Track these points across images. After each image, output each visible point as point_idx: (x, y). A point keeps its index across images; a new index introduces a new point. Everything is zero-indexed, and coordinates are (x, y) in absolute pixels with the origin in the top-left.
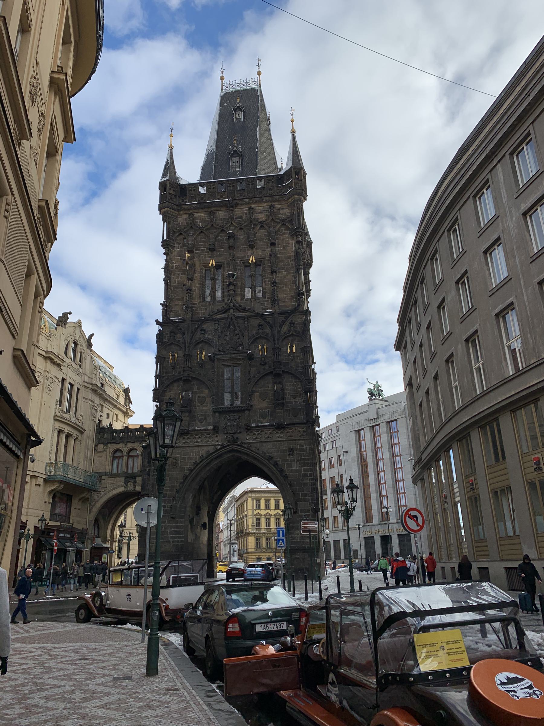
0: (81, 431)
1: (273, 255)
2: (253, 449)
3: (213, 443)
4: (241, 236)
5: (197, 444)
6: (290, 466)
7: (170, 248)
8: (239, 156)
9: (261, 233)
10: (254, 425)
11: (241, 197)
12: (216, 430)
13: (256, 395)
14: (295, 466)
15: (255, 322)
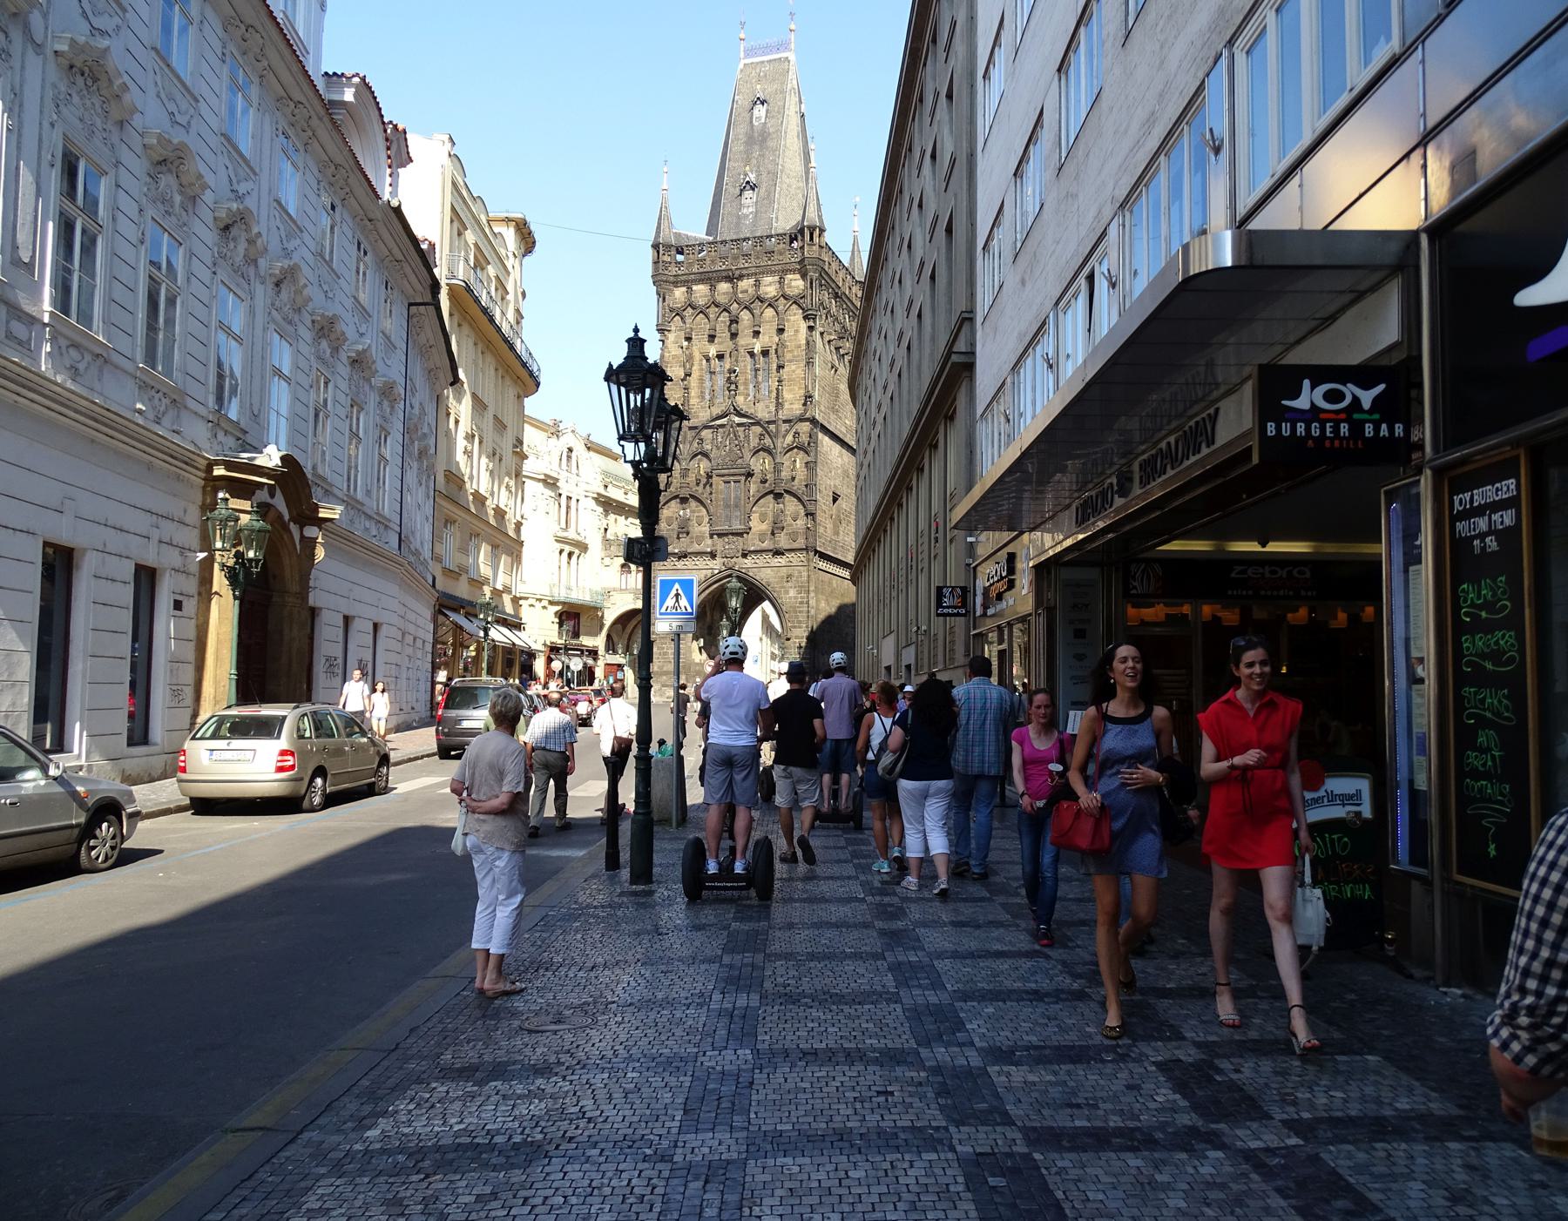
0: (583, 548)
1: (781, 345)
2: (751, 574)
3: (711, 566)
4: (745, 316)
5: (696, 567)
6: (787, 592)
7: (666, 333)
8: (753, 189)
9: (769, 312)
10: (752, 549)
11: (746, 265)
12: (713, 555)
13: (755, 517)
14: (792, 593)
15: (758, 429)
